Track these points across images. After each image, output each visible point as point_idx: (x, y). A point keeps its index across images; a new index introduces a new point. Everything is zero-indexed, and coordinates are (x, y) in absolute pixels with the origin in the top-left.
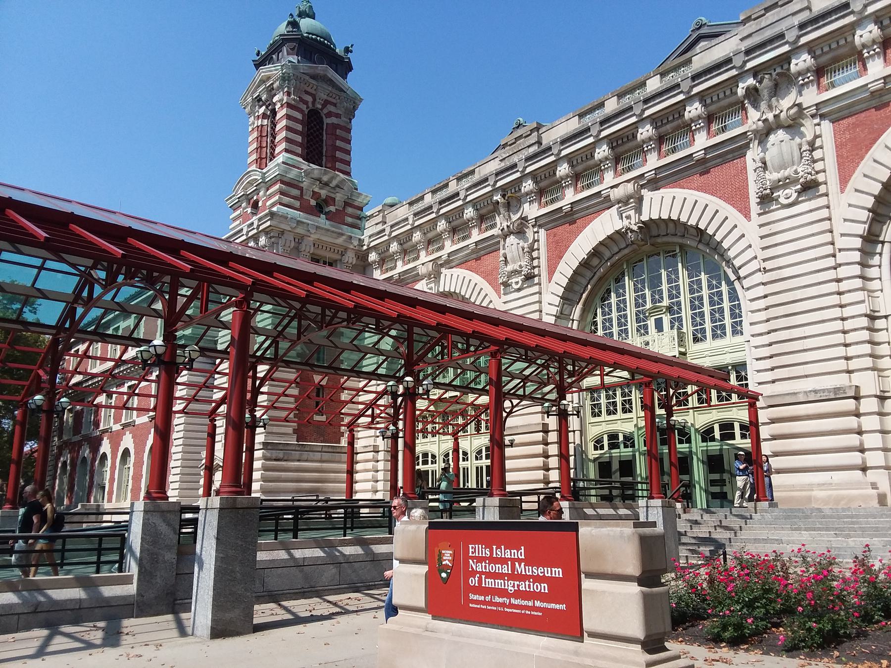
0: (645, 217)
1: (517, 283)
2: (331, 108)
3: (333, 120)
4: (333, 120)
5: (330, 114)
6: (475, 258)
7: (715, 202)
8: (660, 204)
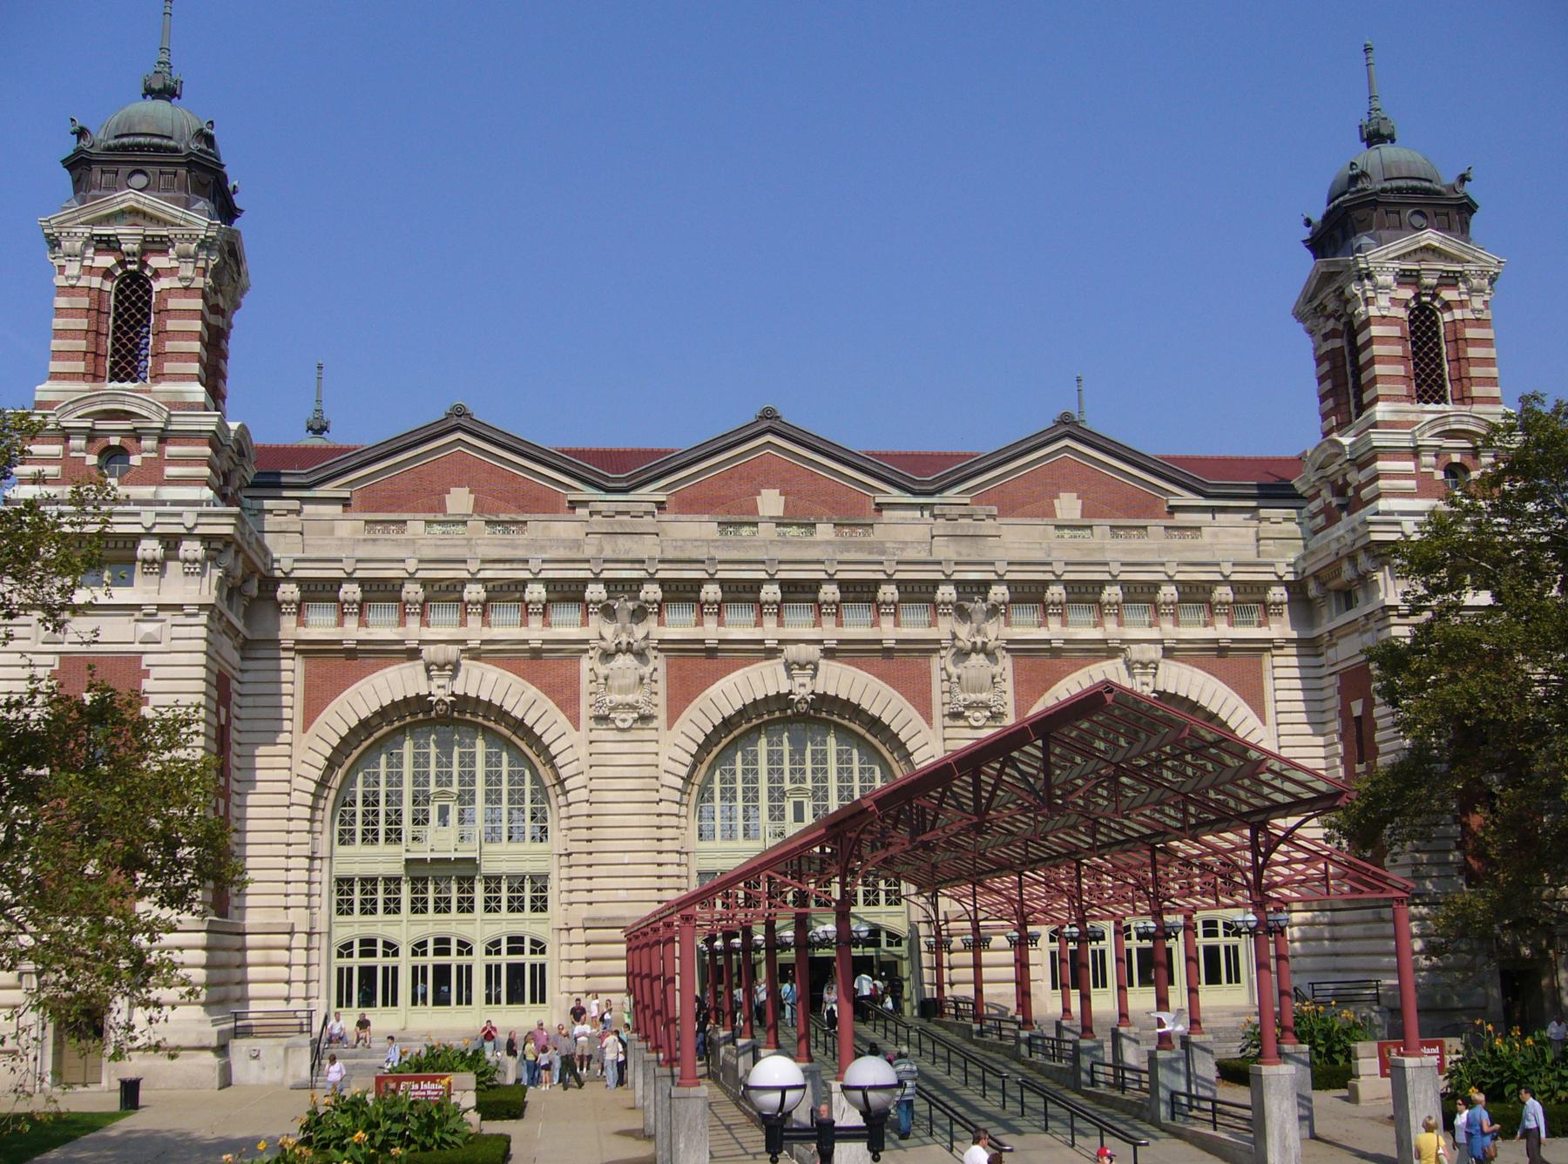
0: (820, 691)
1: (624, 720)
6: (530, 661)
7: (898, 700)
8: (841, 680)
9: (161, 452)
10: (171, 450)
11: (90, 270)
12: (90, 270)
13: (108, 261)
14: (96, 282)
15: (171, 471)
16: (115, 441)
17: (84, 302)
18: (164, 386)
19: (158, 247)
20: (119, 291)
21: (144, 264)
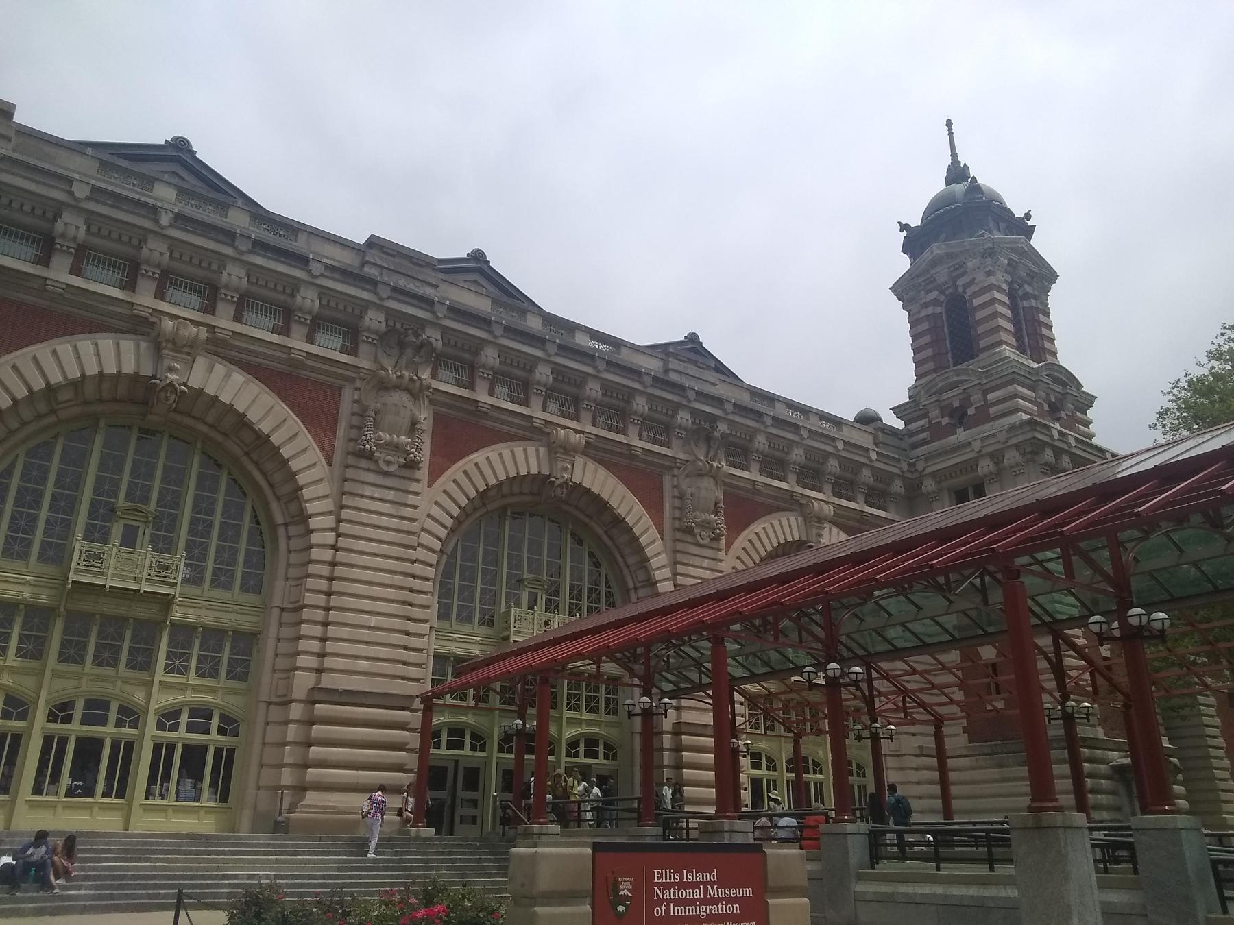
2: (1028, 288)
3: (1034, 303)
4: (1034, 303)
5: (1027, 296)
9: (985, 399)
10: (991, 397)
11: (926, 305)
12: (926, 305)
13: (934, 295)
14: (930, 310)
15: (993, 410)
16: (956, 404)
17: (925, 326)
18: (982, 356)
19: (959, 272)
20: (947, 311)
21: (957, 287)
